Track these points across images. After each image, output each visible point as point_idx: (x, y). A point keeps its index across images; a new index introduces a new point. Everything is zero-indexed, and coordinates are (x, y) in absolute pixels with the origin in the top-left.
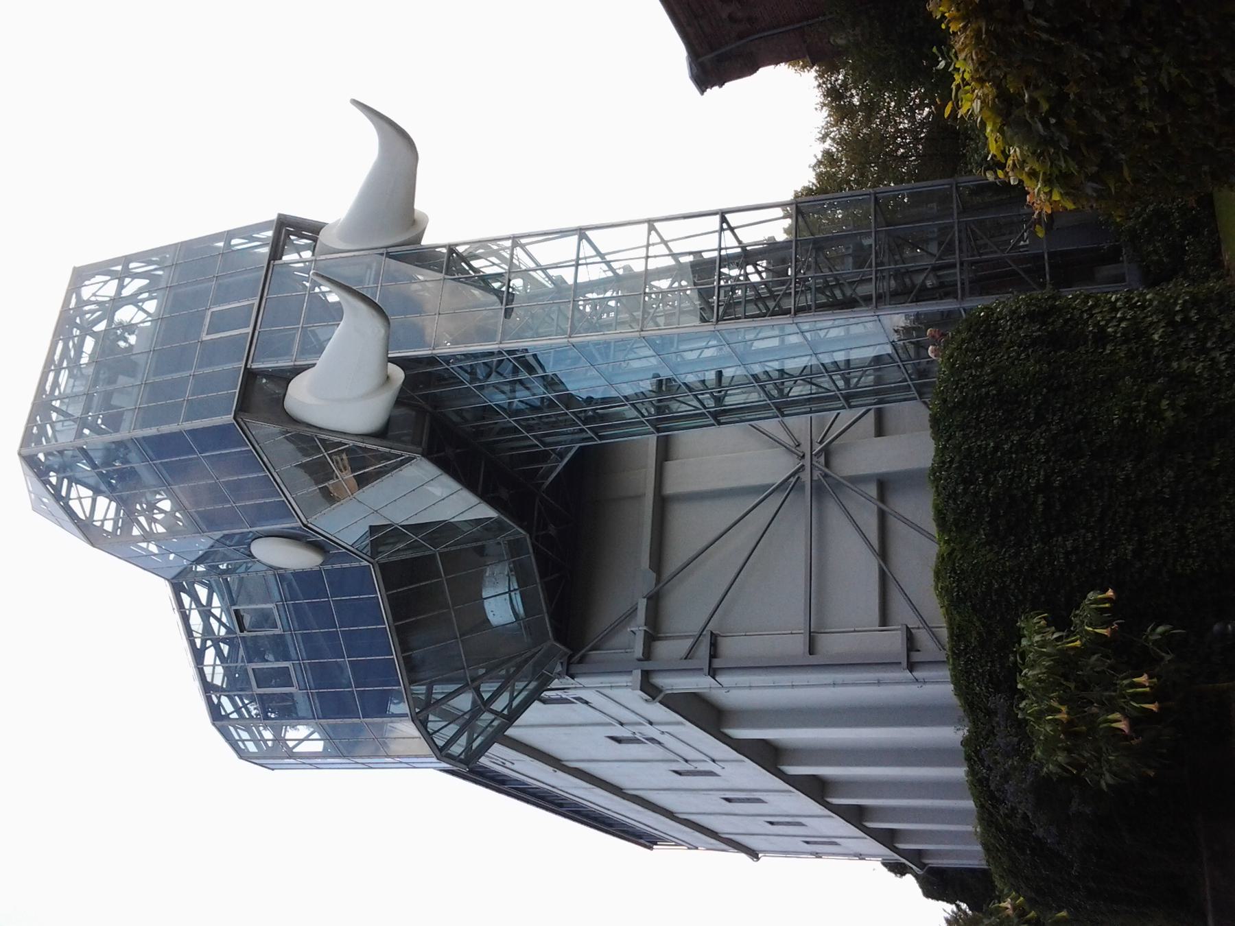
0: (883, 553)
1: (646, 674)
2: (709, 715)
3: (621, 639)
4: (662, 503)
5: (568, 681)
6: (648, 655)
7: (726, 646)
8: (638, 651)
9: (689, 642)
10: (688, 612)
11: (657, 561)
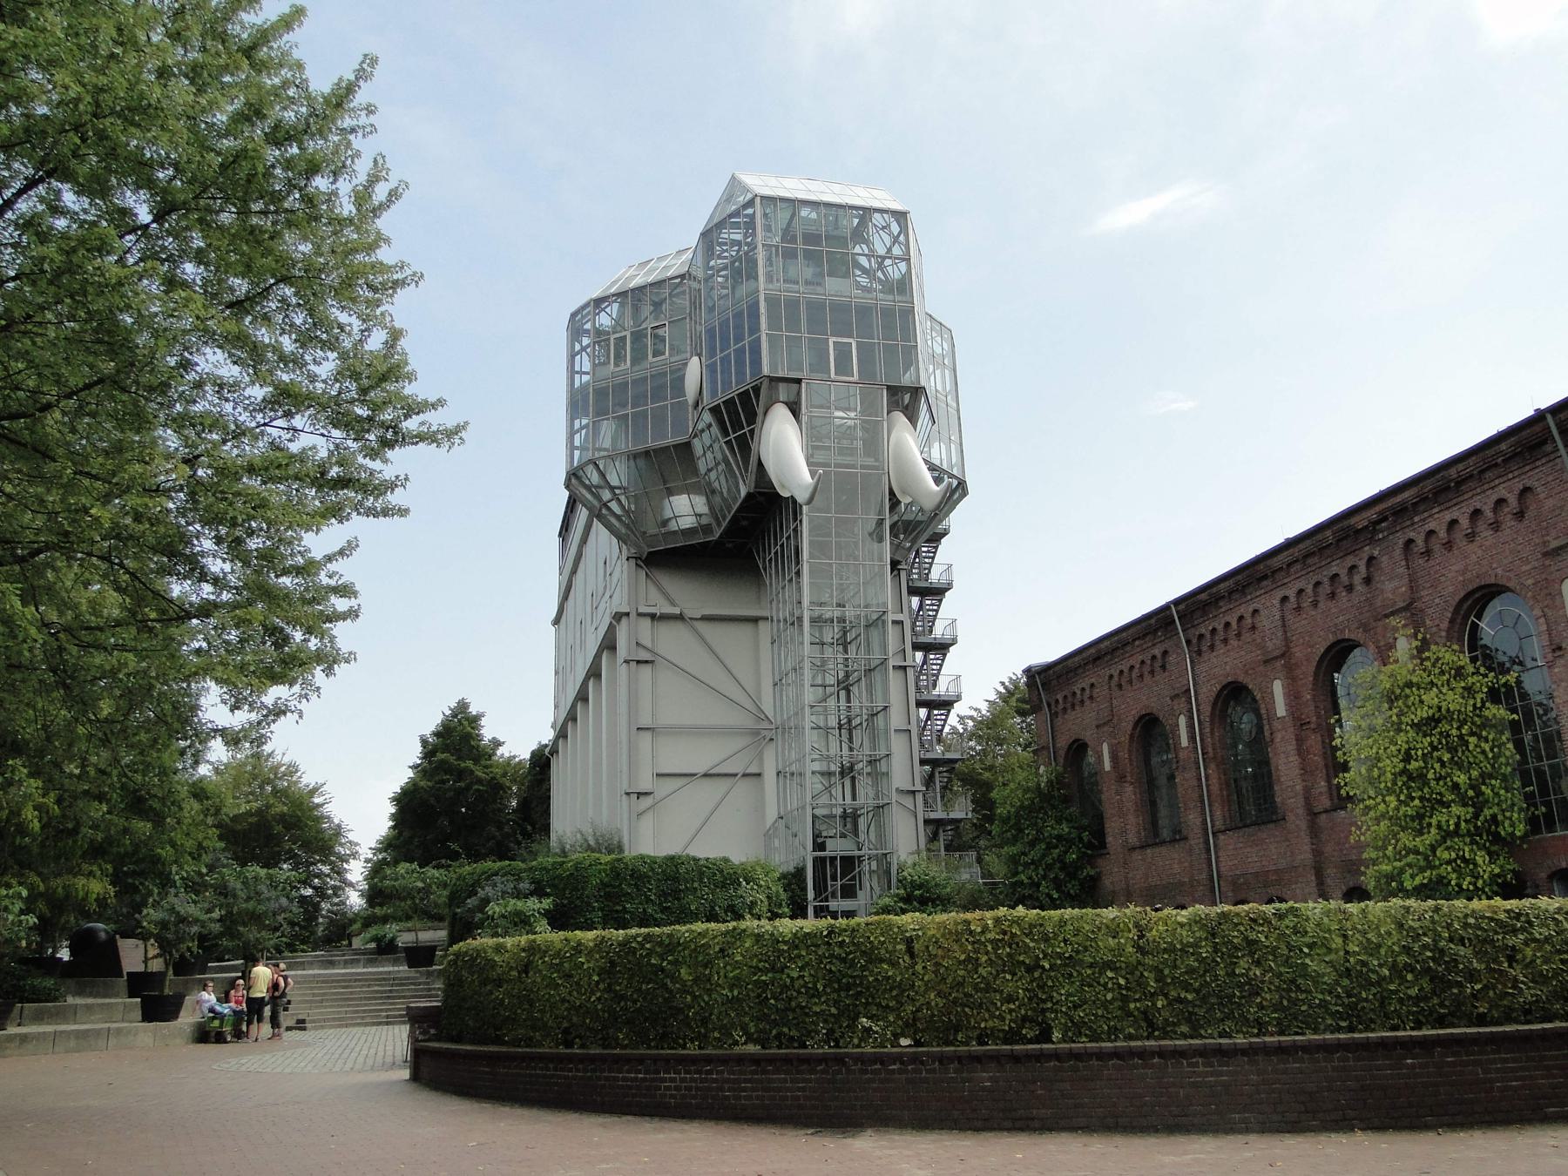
0: (706, 775)
1: (627, 614)
2: (609, 645)
3: (654, 593)
4: (755, 620)
5: (625, 554)
6: (640, 615)
7: (646, 669)
8: (643, 609)
9: (649, 645)
10: (671, 641)
11: (705, 618)
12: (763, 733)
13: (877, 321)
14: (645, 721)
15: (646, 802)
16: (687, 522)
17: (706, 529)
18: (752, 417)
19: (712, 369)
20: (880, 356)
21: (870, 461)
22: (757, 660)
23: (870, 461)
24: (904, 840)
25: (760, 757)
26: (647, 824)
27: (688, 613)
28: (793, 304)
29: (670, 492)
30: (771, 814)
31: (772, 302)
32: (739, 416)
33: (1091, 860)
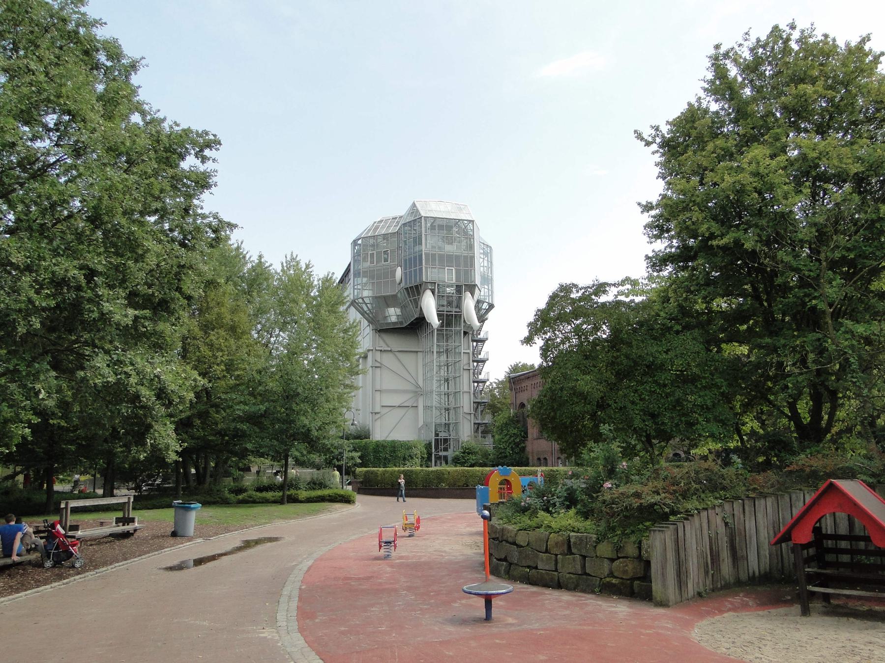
3: (382, 343)
7: (378, 370)
10: (388, 360)
12: (418, 392)
13: (462, 260)
14: (378, 388)
15: (378, 416)
16: (394, 319)
17: (401, 323)
18: (419, 294)
19: (406, 274)
20: (462, 273)
21: (458, 310)
22: (417, 363)
23: (458, 310)
24: (465, 433)
25: (417, 400)
26: (378, 423)
27: (393, 349)
28: (434, 255)
29: (388, 306)
30: (421, 423)
31: (427, 255)
32: (415, 291)
33: (524, 442)
